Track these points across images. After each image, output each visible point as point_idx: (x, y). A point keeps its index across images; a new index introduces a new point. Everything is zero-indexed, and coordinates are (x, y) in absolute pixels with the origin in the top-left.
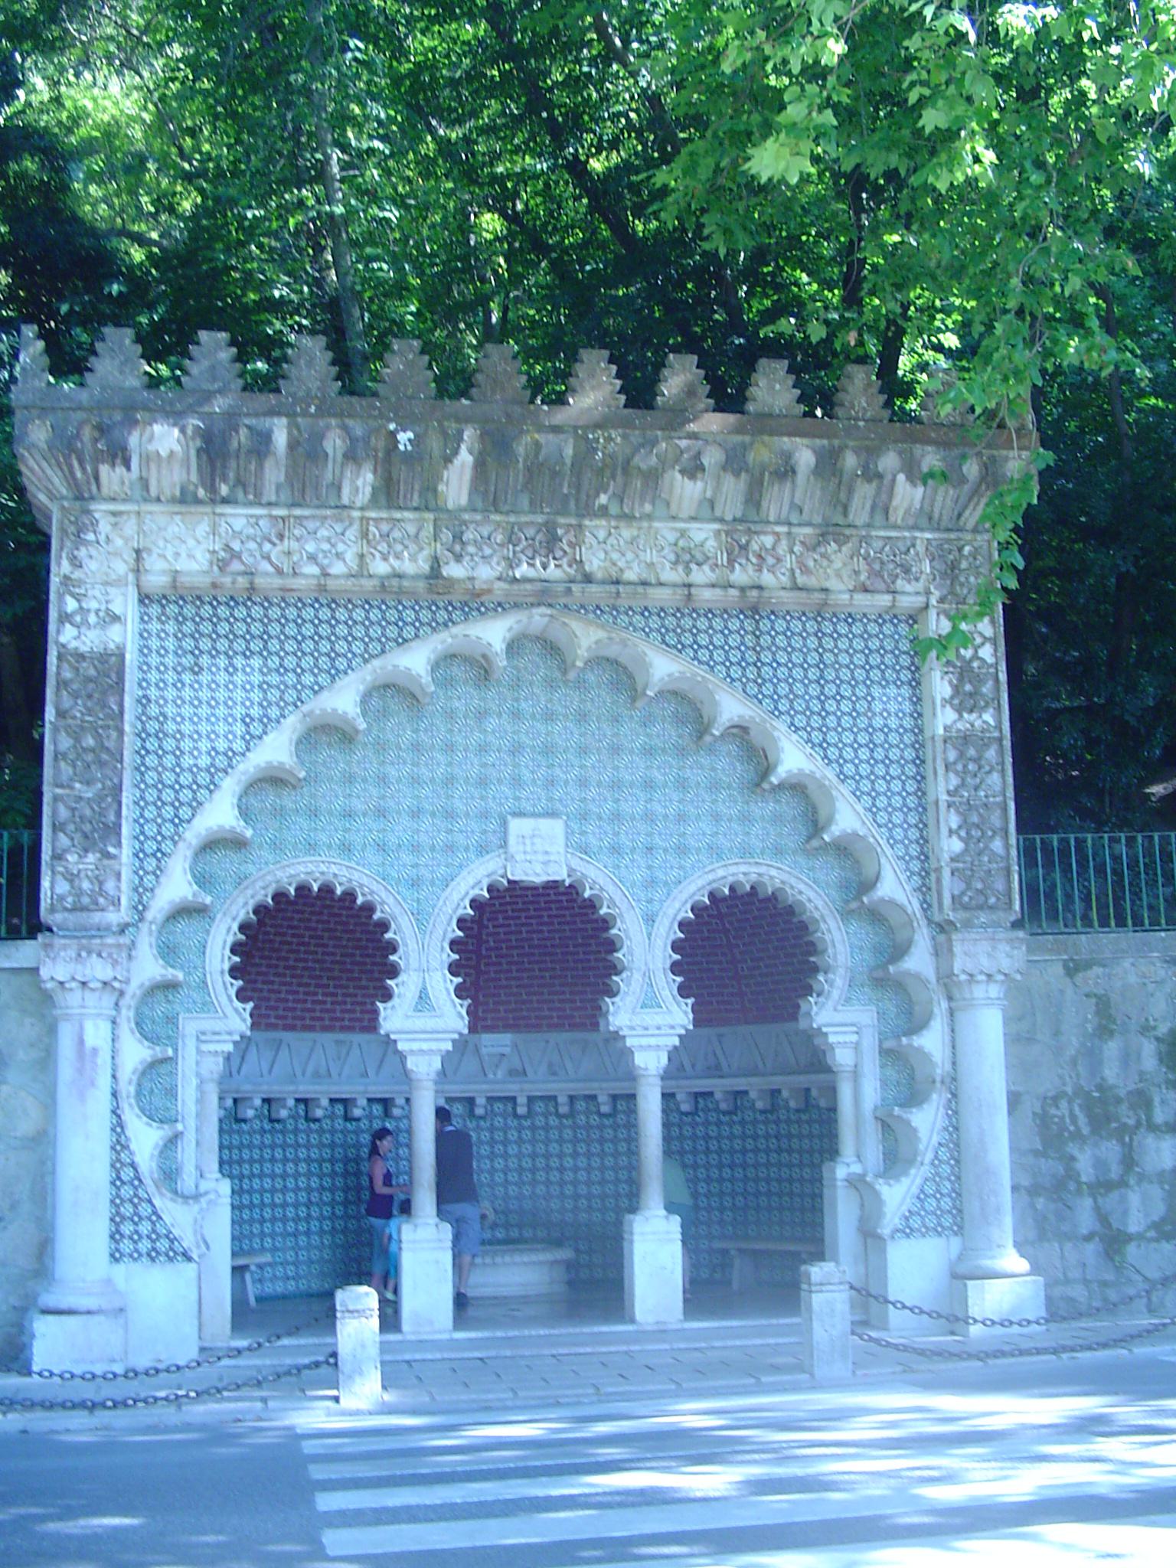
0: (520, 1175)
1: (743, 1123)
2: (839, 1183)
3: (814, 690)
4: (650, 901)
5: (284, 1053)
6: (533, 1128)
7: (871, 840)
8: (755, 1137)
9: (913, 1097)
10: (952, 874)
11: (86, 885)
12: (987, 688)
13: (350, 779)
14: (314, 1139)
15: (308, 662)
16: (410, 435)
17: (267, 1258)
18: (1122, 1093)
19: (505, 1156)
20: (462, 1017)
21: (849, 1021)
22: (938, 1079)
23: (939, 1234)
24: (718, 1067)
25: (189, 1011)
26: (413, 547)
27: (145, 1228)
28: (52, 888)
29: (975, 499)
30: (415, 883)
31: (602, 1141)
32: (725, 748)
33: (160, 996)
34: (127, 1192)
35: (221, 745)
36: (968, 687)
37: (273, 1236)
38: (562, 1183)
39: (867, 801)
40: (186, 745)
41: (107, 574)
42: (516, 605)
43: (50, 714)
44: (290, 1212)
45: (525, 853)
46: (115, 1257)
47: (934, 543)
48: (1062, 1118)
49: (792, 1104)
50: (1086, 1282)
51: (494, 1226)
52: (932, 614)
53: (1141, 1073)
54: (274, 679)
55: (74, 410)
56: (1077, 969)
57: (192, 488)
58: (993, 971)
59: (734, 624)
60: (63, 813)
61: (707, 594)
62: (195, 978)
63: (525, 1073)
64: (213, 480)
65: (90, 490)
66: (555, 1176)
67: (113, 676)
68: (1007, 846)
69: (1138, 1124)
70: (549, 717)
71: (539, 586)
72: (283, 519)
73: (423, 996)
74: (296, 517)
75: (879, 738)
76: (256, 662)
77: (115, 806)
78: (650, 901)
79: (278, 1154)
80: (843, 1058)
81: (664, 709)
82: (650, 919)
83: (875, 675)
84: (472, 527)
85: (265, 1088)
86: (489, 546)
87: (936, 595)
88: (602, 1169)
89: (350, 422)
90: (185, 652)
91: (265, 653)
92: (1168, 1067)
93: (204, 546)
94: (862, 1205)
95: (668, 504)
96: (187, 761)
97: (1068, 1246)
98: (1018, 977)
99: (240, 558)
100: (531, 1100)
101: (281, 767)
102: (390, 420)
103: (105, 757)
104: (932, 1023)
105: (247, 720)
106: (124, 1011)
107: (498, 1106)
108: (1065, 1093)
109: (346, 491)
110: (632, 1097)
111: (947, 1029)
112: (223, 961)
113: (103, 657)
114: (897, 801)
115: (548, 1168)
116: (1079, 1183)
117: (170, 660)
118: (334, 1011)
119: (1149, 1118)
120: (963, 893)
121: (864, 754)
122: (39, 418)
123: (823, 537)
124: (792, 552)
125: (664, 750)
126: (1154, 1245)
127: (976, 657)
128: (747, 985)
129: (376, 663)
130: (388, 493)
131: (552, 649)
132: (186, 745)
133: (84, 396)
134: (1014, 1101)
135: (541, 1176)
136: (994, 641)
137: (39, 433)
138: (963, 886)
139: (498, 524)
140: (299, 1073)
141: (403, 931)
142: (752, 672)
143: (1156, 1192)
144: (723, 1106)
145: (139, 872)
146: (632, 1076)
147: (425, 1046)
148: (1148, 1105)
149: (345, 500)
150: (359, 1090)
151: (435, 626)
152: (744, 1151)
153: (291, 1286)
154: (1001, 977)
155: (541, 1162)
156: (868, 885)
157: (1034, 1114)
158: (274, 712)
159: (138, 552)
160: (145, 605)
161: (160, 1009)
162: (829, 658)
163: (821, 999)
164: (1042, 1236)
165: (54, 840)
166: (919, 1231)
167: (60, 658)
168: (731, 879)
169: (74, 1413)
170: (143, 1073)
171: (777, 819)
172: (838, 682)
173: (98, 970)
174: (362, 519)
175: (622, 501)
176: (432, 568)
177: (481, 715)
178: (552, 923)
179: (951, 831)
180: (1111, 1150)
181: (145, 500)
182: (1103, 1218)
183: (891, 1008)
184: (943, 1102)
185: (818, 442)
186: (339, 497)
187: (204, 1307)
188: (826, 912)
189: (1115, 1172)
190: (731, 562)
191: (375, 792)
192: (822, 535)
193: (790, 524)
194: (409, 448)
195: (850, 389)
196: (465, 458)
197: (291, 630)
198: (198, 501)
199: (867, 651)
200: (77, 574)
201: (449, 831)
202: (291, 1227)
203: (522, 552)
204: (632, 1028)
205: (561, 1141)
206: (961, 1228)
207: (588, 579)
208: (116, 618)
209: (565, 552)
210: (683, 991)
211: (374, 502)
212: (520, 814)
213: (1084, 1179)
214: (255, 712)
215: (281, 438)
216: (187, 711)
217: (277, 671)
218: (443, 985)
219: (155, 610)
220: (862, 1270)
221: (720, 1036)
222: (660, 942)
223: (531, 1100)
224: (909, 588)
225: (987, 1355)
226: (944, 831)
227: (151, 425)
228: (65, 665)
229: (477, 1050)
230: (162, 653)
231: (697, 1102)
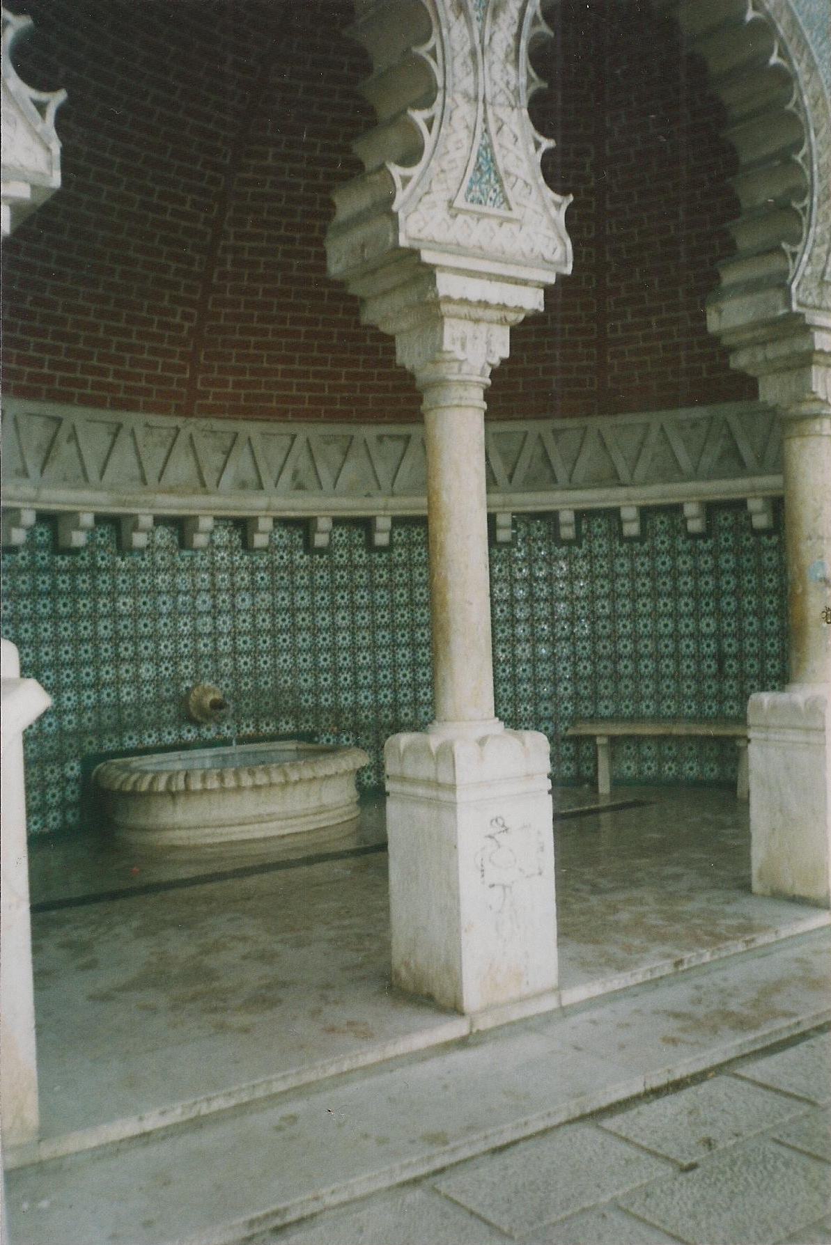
31: (372, 586)
38: (314, 650)
63: (260, 486)
66: (303, 640)
88: (374, 627)
135: (284, 640)
155: (283, 621)
205: (312, 588)
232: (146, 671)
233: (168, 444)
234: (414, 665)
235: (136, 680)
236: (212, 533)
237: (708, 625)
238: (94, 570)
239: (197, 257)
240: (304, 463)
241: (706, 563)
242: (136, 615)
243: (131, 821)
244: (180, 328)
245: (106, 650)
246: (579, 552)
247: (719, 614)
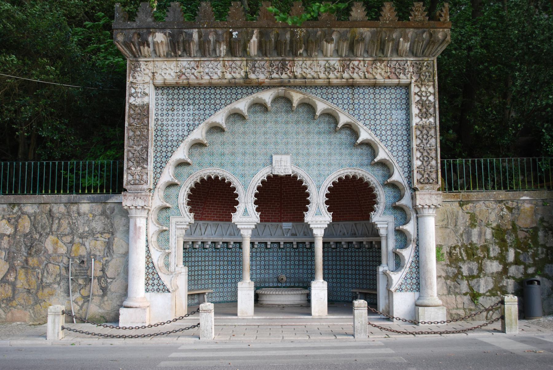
0: (295, 266)
1: (362, 252)
2: (380, 273)
3: (372, 112)
4: (319, 181)
5: (219, 226)
6: (299, 252)
7: (391, 161)
8: (366, 256)
9: (405, 246)
10: (417, 172)
11: (137, 177)
12: (431, 110)
13: (223, 143)
14: (229, 254)
15: (207, 107)
16: (237, 33)
17: (210, 291)
18: (479, 246)
19: (290, 260)
20: (258, 218)
21: (385, 220)
22: (412, 240)
23: (412, 291)
24: (355, 234)
25: (173, 215)
26: (239, 69)
27: (156, 282)
28: (127, 178)
29: (428, 46)
30: (243, 176)
32: (343, 132)
33: (164, 211)
34: (151, 271)
35: (181, 133)
36: (424, 110)
37: (216, 283)
38: (307, 269)
39: (390, 148)
40: (170, 133)
41: (144, 81)
42: (274, 87)
43: (126, 125)
44: (221, 277)
45: (278, 166)
46: (147, 291)
47: (414, 62)
48: (457, 253)
49: (376, 246)
50: (464, 309)
51: (286, 282)
52: (413, 85)
53: (486, 240)
54: (197, 112)
55: (132, 29)
56: (463, 205)
57: (170, 53)
58: (430, 204)
59: (346, 91)
60: (131, 155)
61: (335, 81)
62: (175, 205)
64: (175, 50)
65: (138, 55)
66: (305, 267)
67: (146, 113)
68: (437, 163)
69: (484, 257)
70: (287, 123)
71: (279, 80)
72: (198, 61)
73: (246, 211)
74: (202, 61)
75: (394, 127)
76: (191, 107)
77: (146, 153)
78: (319, 181)
79: (218, 259)
80: (382, 232)
81: (324, 119)
82: (319, 187)
83: (393, 106)
84: (258, 62)
85: (212, 239)
86: (264, 68)
87: (414, 79)
89: (218, 30)
90: (169, 104)
91: (194, 104)
92: (496, 238)
93: (174, 71)
94: (388, 280)
95: (322, 52)
96: (170, 138)
97: (458, 296)
98: (439, 206)
99: (184, 74)
100: (298, 243)
101: (199, 140)
102: (230, 28)
103: (143, 137)
104: (410, 221)
105: (188, 125)
106: (150, 216)
107: (288, 245)
108: (458, 246)
109: (218, 52)
110: (314, 243)
111: (416, 224)
112: (183, 200)
113: (143, 106)
114: (400, 148)
115: (303, 265)
116: (462, 276)
117: (165, 107)
118: (266, 213)
119: (488, 254)
120: (421, 179)
121: (389, 133)
122: (121, 32)
123: (375, 61)
124: (364, 66)
125: (324, 133)
126: (488, 298)
127: (427, 99)
128: (363, 208)
129: (228, 106)
130: (231, 52)
131: (289, 101)
132: (170, 133)
133: (134, 25)
134: (439, 248)
135: (301, 267)
136: (434, 94)
137: (120, 38)
138: (421, 176)
139: (266, 60)
140: (224, 234)
141: (240, 190)
142: (351, 107)
143: (490, 279)
144: (356, 246)
145: (155, 173)
146: (313, 236)
147: (246, 227)
148: (488, 251)
149: (218, 55)
150: (231, 240)
151: (248, 94)
152: (363, 261)
153: (221, 299)
154: (434, 207)
155: (301, 263)
156: (390, 176)
157: (447, 252)
158: (197, 122)
159: (153, 73)
160: (158, 90)
161: (165, 214)
162: (377, 101)
163: (375, 213)
164: (449, 293)
165: (128, 164)
166: (405, 289)
167: (130, 107)
168: (345, 174)
169: (119, 339)
170: (159, 234)
171: (361, 155)
172: (381, 109)
173: (140, 203)
174: (223, 60)
175: (307, 52)
176: (245, 75)
177: (265, 122)
179: (417, 158)
180: (474, 265)
181: (156, 57)
182: (471, 288)
183: (399, 217)
184: (414, 247)
185: (373, 29)
186: (216, 54)
187: (177, 306)
188: (377, 185)
189: (475, 273)
190: (344, 72)
191: (231, 147)
192: (375, 60)
193: (364, 57)
194: (236, 37)
195: (384, 11)
196: (254, 39)
197: (202, 97)
198: (172, 57)
199: (390, 98)
200: (135, 81)
201: (254, 159)
202: (221, 281)
203: (274, 69)
204: (312, 222)
206: (419, 289)
207: (295, 77)
208: (146, 94)
209: (288, 69)
210: (329, 210)
211: (227, 55)
212: (277, 154)
213: (464, 274)
214: (191, 122)
215: (195, 36)
216: (170, 123)
217: (198, 109)
218: (252, 208)
219: (160, 91)
220: (387, 301)
221: (355, 224)
222: (322, 194)
223: (298, 243)
224: (404, 77)
225: (416, 333)
226: (415, 158)
227: (155, 33)
228: (131, 109)
229: (281, 227)
230: (162, 105)
231: (349, 245)
232: (271, 271)
235: (269, 274)
238: (261, 252)
242: (269, 261)
243: (262, 299)
244: (277, 206)
246: (360, 250)
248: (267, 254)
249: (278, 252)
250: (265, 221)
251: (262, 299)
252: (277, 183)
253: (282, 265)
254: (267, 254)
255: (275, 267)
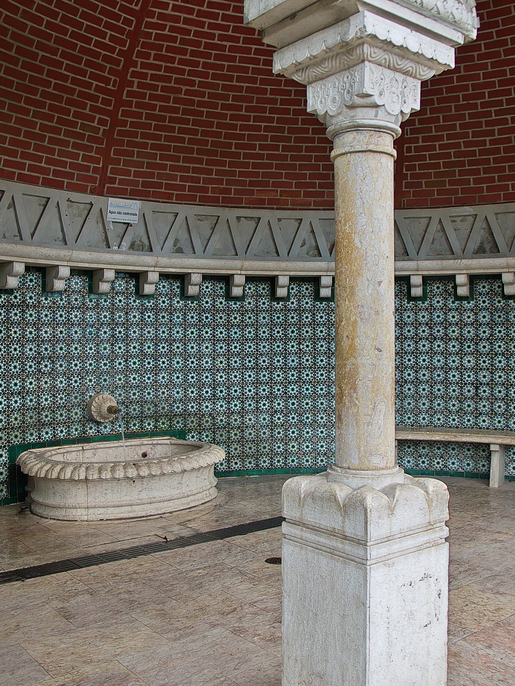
19: (127, 340)
31: (228, 325)
38: (185, 371)
66: (178, 362)
88: (229, 355)
178: (205, 75)
205: (185, 325)
232: (61, 383)
233: (84, 217)
234: (257, 383)
236: (113, 282)
237: (469, 361)
238: (24, 306)
239: (113, 78)
240: (183, 235)
241: (469, 317)
242: (54, 340)
245: (31, 366)
247: (477, 353)
248: (45, 315)
249: (83, 308)
250: (48, 184)
251: (50, 501)
252: (121, 31)
253: (98, 357)
254: (45, 315)
255: (76, 366)
